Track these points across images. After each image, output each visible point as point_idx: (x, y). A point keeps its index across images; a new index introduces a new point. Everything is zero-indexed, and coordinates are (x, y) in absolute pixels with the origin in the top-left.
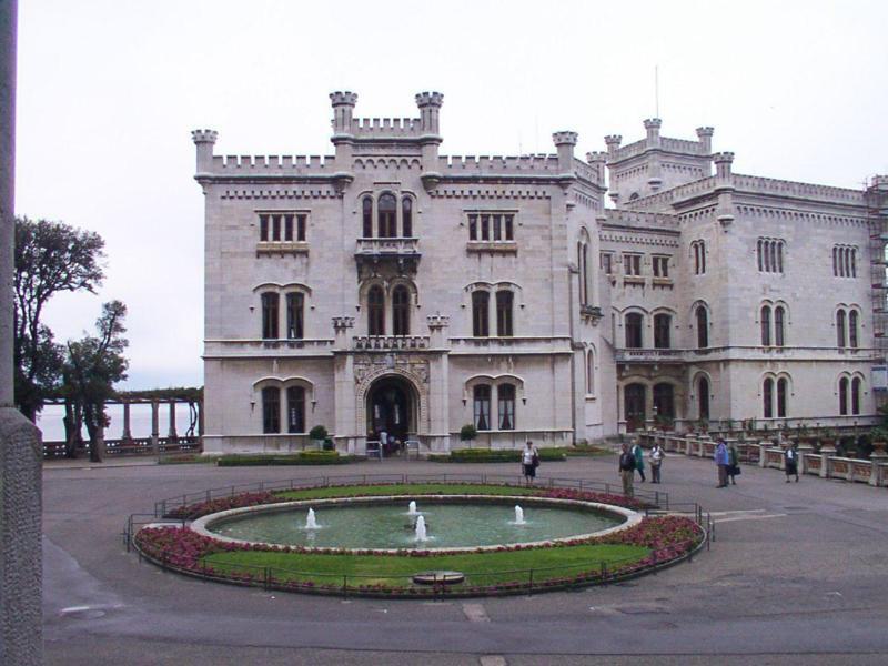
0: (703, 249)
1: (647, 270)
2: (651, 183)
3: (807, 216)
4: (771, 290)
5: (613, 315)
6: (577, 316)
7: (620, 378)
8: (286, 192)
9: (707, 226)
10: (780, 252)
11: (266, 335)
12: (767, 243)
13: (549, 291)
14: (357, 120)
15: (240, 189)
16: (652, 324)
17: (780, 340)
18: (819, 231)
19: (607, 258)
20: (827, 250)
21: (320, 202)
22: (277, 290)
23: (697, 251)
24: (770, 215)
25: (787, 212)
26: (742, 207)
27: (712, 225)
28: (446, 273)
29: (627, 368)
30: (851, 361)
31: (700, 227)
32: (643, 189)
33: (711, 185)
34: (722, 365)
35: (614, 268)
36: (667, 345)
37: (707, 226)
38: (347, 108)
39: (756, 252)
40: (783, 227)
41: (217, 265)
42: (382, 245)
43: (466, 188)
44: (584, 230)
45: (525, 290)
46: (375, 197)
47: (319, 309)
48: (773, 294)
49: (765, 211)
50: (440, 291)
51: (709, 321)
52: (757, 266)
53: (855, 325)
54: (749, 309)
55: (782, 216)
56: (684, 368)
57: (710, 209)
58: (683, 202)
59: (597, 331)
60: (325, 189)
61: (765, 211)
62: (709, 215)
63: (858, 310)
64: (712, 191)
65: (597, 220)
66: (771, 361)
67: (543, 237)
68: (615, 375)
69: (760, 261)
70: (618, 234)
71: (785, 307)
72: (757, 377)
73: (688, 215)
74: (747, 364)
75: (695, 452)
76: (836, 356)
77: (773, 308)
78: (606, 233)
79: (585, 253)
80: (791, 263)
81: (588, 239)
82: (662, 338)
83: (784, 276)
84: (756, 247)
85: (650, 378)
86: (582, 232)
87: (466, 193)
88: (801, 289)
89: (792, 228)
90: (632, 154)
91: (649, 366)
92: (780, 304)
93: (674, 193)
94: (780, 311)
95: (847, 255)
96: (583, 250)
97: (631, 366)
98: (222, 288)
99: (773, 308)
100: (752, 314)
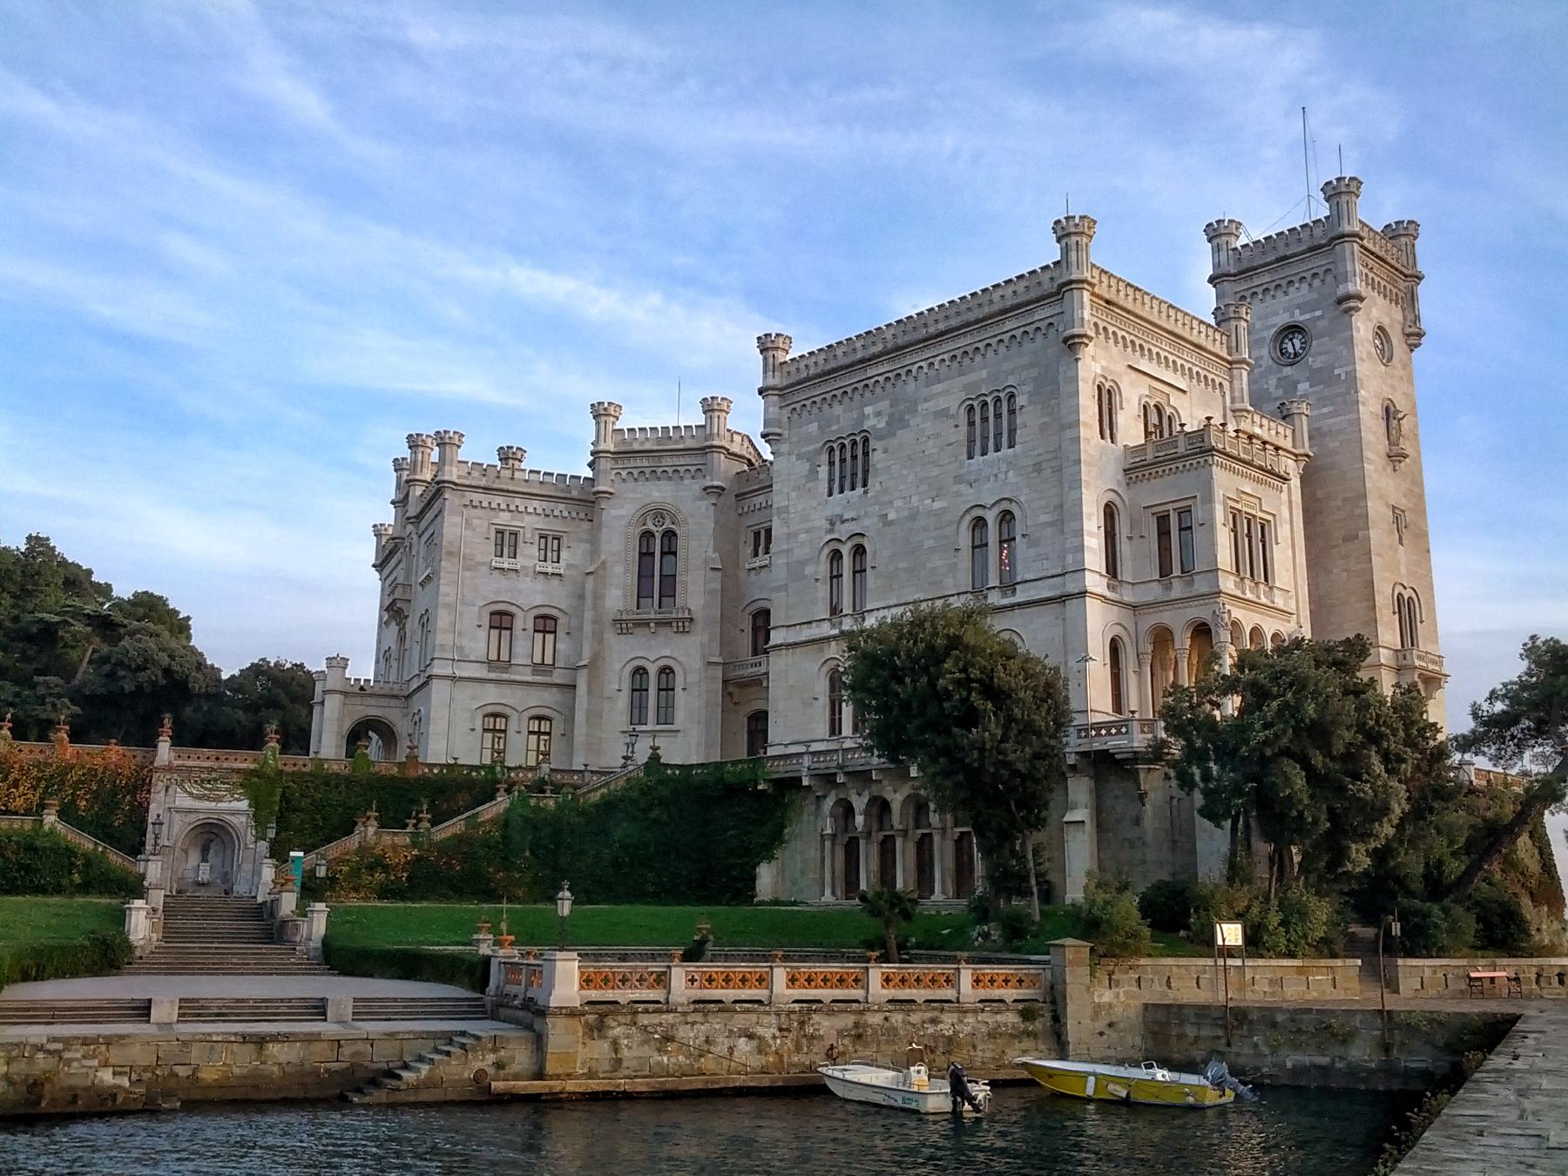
4: (843, 522)
10: (866, 454)
12: (843, 446)
18: (937, 388)
39: (823, 471)
40: (868, 410)
48: (846, 525)
52: (824, 487)
63: (1014, 508)
65: (705, 489)
69: (831, 481)
77: (846, 550)
80: (879, 466)
83: (866, 492)
84: (825, 457)
89: (884, 405)
94: (859, 551)
100: (809, 570)
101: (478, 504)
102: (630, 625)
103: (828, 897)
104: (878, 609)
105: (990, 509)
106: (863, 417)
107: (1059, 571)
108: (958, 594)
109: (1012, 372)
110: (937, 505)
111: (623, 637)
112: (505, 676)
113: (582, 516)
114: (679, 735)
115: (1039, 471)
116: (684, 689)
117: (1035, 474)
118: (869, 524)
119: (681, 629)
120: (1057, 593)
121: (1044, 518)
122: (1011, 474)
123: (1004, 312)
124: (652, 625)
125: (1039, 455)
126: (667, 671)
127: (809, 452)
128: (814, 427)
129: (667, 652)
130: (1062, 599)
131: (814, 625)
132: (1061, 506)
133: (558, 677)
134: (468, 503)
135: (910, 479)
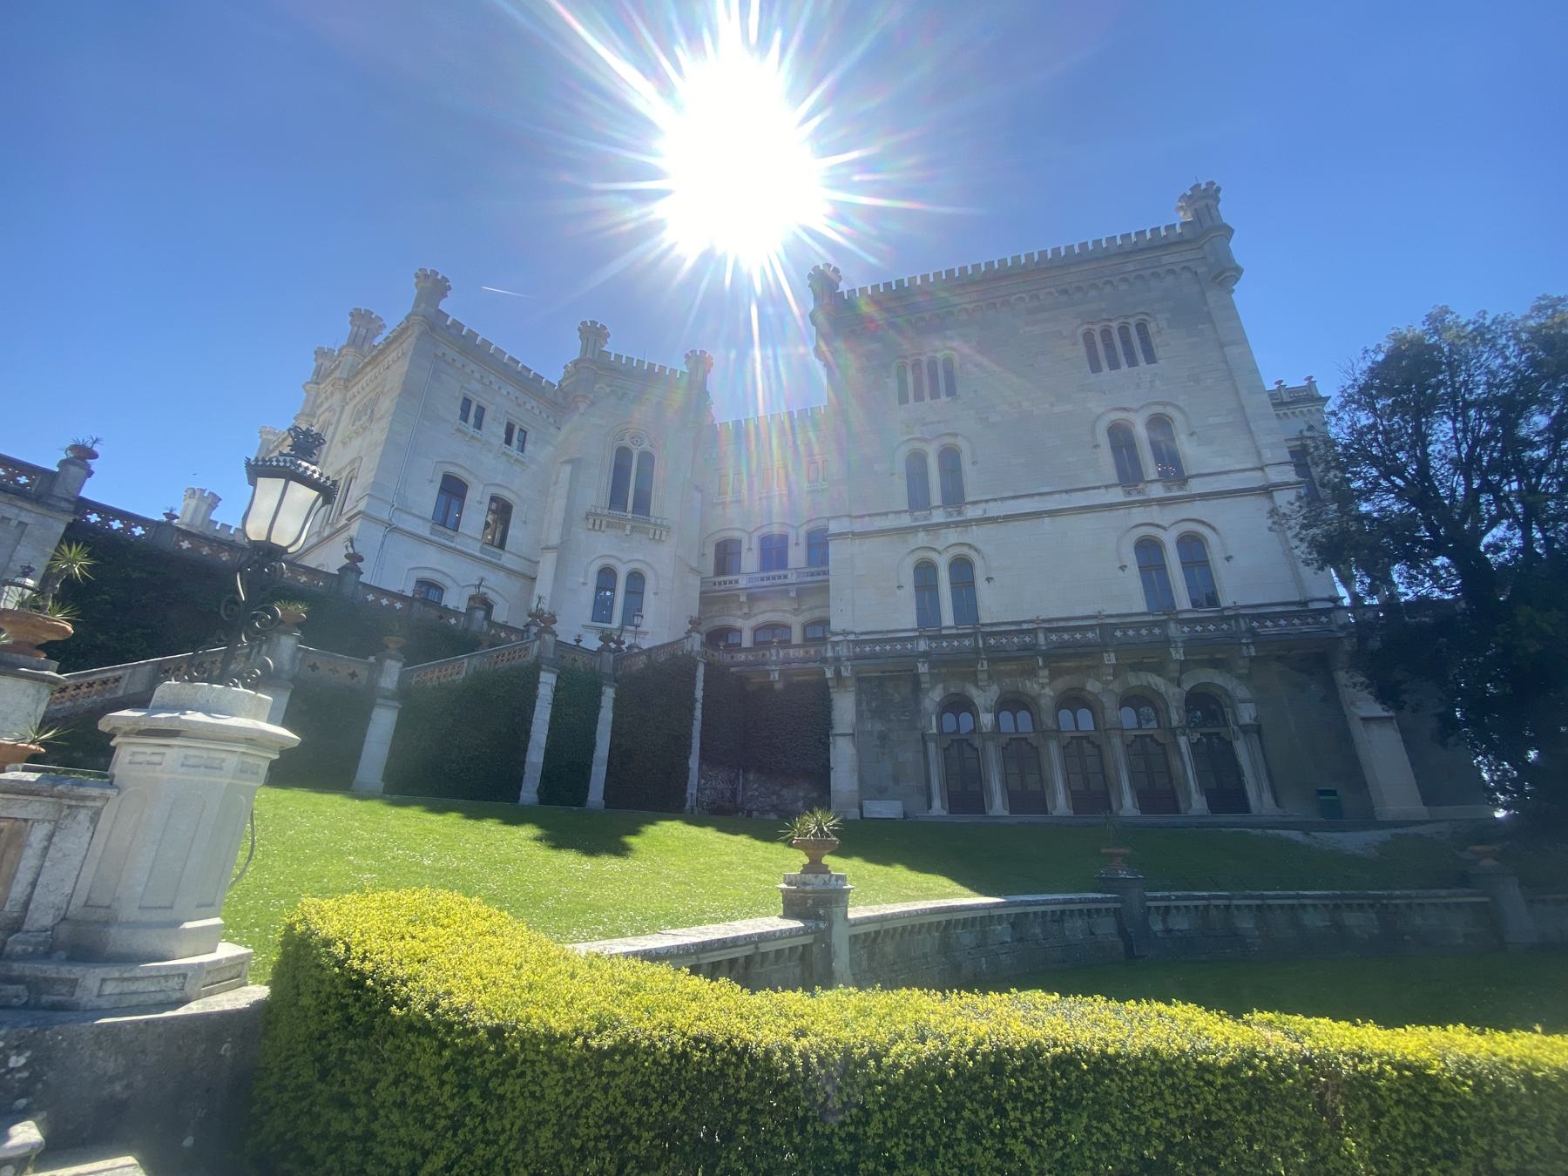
17: (954, 497)
30: (1161, 502)
63: (1170, 411)
66: (928, 528)
72: (899, 562)
85: (796, 611)
101: (450, 360)
102: (604, 523)
103: (938, 808)
104: (987, 501)
105: (1136, 411)
108: (1107, 487)
111: (593, 533)
112: (448, 543)
113: (551, 420)
116: (656, 594)
119: (657, 537)
122: (1158, 383)
124: (628, 527)
126: (636, 579)
129: (641, 557)
131: (891, 517)
132: (1243, 407)
133: (507, 559)
134: (440, 354)
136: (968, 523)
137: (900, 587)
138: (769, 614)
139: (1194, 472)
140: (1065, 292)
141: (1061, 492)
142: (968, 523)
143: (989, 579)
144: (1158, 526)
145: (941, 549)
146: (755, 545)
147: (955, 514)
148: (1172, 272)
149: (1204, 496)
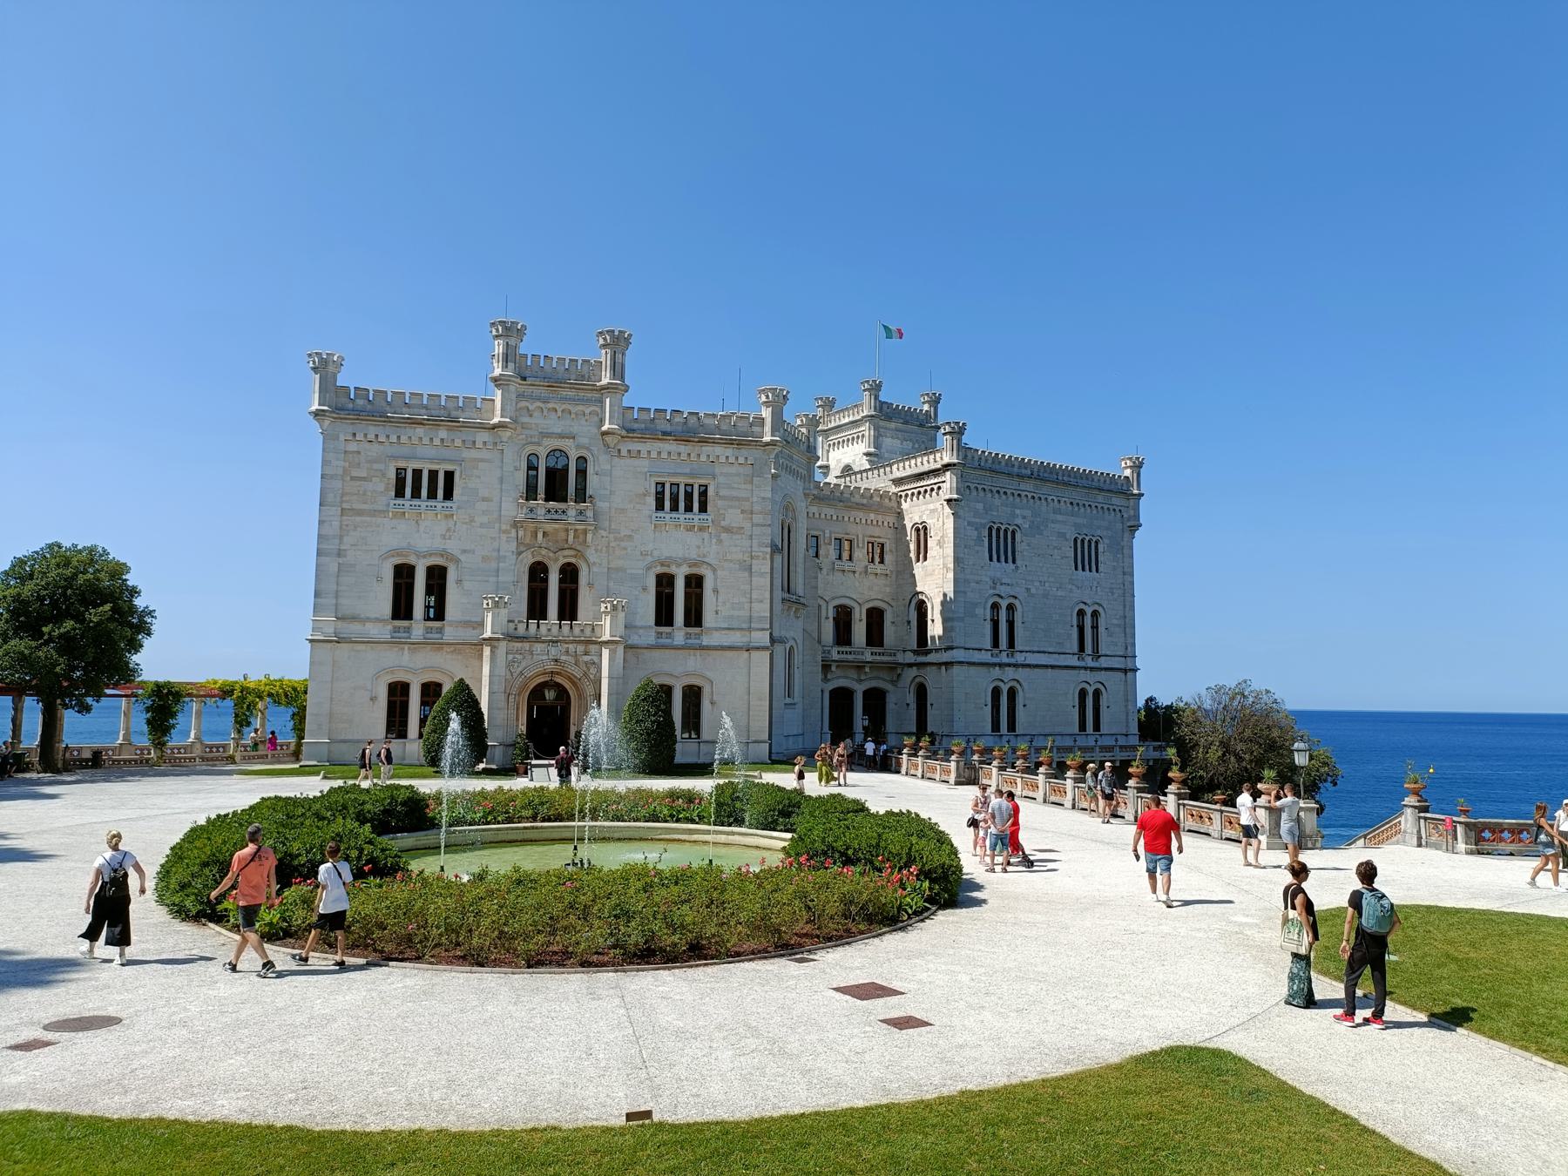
0: (926, 534)
1: (860, 554)
2: (865, 454)
3: (1046, 499)
4: (1002, 584)
5: (820, 606)
6: (778, 606)
7: (825, 680)
8: (431, 439)
9: (931, 506)
11: (396, 615)
12: (998, 530)
13: (746, 574)
14: (526, 356)
15: (372, 431)
16: (864, 617)
17: (1011, 644)
18: (1059, 517)
19: (815, 542)
20: (1067, 540)
21: (473, 454)
22: (412, 560)
23: (918, 535)
24: (1004, 497)
25: (1023, 494)
26: (972, 486)
27: (938, 505)
28: (625, 549)
29: (833, 668)
30: (1092, 669)
31: (924, 507)
32: (857, 460)
33: (938, 459)
34: (943, 667)
35: (821, 552)
36: (881, 644)
37: (931, 506)
38: (512, 342)
39: (986, 540)
40: (1018, 512)
41: (336, 524)
42: (549, 511)
43: (654, 447)
44: (788, 508)
45: (719, 572)
46: (542, 452)
47: (467, 585)
49: (998, 492)
50: (618, 570)
51: (929, 617)
53: (1097, 627)
54: (975, 605)
55: (1018, 500)
56: (899, 671)
57: (935, 487)
58: (902, 479)
59: (800, 623)
60: (482, 437)
61: (998, 492)
62: (934, 493)
63: (1101, 610)
64: (938, 466)
66: (1001, 665)
67: (743, 512)
68: (820, 676)
70: (829, 511)
71: (1017, 603)
72: (983, 682)
73: (909, 492)
74: (972, 669)
75: (912, 772)
76: (1074, 661)
78: (814, 509)
79: (789, 532)
80: (1025, 553)
81: (795, 518)
82: (875, 634)
83: (1017, 568)
86: (786, 508)
87: (654, 455)
88: (1037, 584)
89: (1028, 513)
90: (847, 420)
91: (859, 667)
92: (1012, 600)
93: (895, 467)
95: (1090, 546)
96: (787, 531)
97: (837, 667)
98: (340, 553)
99: (1004, 604)
100: (980, 611)
106: (1014, 515)
107: (1121, 653)
109: (1099, 527)
110: (1059, 593)
114: (796, 706)
115: (1113, 594)
117: (1110, 594)
118: (1019, 591)
120: (1123, 666)
121: (1115, 622)
123: (1101, 490)
125: (1112, 583)
127: (977, 523)
128: (980, 506)
130: (1125, 671)
132: (1125, 617)
135: (1044, 569)
136: (1015, 665)
137: (986, 705)
138: (841, 680)
139: (1103, 653)
140: (1072, 503)
141: (1055, 653)
142: (1015, 665)
143: (1024, 706)
144: (1088, 683)
145: (1006, 681)
146: (831, 614)
147: (1010, 655)
148: (1114, 510)
149: (1106, 669)
